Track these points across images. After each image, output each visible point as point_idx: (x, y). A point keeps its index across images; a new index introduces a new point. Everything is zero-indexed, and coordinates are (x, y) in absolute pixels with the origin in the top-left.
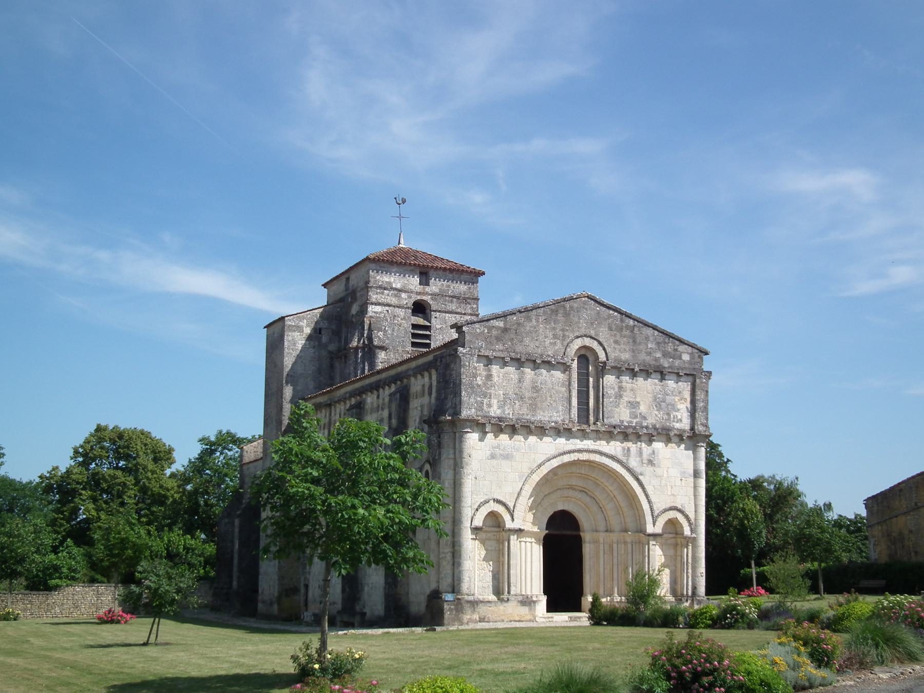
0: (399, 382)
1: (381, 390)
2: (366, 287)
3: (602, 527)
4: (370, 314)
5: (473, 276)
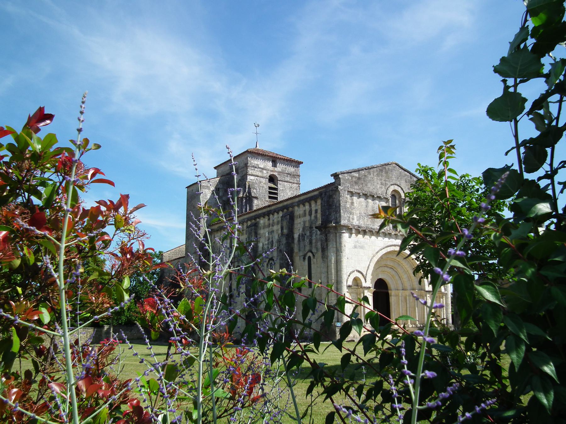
0: (285, 210)
1: (271, 216)
2: (246, 166)
3: (401, 288)
4: (248, 180)
5: (297, 164)
